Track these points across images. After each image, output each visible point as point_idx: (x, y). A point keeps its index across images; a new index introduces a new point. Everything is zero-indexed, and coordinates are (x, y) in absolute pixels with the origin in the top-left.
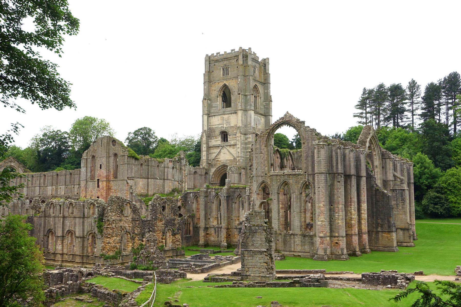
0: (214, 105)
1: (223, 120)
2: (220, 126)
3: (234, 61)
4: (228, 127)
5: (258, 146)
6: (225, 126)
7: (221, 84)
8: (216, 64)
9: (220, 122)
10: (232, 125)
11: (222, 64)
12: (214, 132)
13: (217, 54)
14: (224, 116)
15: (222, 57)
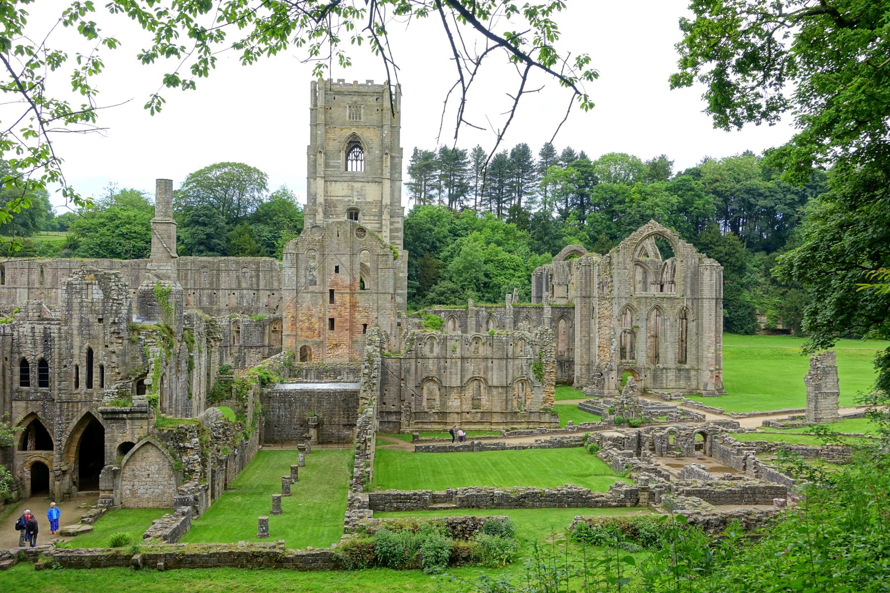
0: (332, 162)
1: (352, 190)
2: (347, 199)
3: (371, 100)
4: (361, 203)
5: (621, 260)
6: (355, 199)
7: (348, 133)
8: (336, 97)
9: (346, 192)
10: (370, 199)
11: (348, 100)
12: (335, 206)
13: (339, 80)
14: (354, 184)
15: (350, 89)
